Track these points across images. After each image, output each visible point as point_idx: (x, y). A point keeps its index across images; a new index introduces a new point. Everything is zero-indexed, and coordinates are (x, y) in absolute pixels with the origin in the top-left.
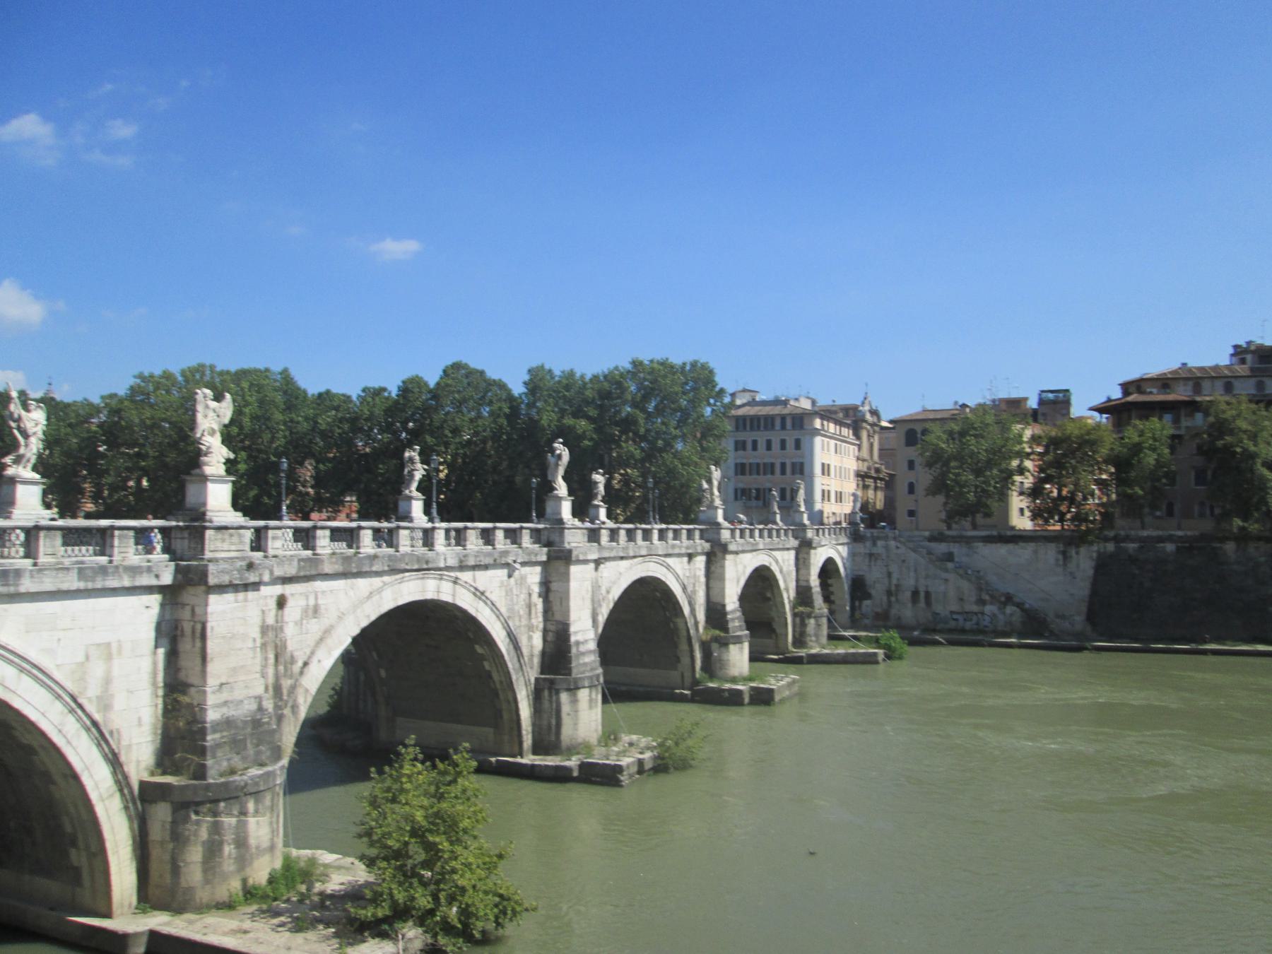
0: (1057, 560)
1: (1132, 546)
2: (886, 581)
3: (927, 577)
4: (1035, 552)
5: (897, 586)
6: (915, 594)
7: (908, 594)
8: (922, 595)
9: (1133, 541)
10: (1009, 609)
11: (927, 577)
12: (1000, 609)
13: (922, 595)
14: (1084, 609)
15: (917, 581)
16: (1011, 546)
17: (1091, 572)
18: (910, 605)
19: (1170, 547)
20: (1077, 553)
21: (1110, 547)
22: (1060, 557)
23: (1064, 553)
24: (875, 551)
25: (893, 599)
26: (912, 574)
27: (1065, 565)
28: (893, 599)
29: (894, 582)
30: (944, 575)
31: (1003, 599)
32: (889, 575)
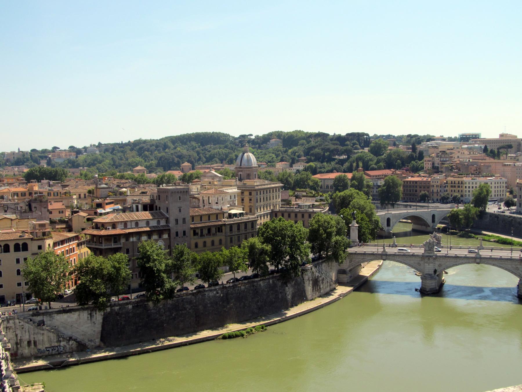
0: (88, 317)
1: (117, 308)
2: (15, 338)
3: (34, 334)
4: (79, 315)
5: (20, 340)
6: (29, 343)
7: (26, 343)
8: (32, 342)
9: (117, 306)
10: (71, 343)
11: (34, 334)
12: (67, 343)
13: (32, 342)
14: (100, 336)
15: (30, 336)
16: (69, 314)
17: (101, 321)
18: (27, 347)
19: (130, 307)
20: (96, 314)
21: (109, 309)
22: (89, 316)
23: (90, 314)
24: (9, 325)
25: (19, 346)
26: (27, 333)
27: (91, 319)
28: (19, 346)
29: (19, 338)
30: (42, 332)
31: (68, 338)
32: (16, 335)
